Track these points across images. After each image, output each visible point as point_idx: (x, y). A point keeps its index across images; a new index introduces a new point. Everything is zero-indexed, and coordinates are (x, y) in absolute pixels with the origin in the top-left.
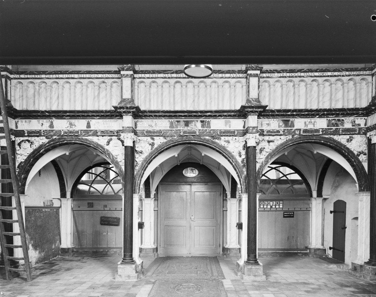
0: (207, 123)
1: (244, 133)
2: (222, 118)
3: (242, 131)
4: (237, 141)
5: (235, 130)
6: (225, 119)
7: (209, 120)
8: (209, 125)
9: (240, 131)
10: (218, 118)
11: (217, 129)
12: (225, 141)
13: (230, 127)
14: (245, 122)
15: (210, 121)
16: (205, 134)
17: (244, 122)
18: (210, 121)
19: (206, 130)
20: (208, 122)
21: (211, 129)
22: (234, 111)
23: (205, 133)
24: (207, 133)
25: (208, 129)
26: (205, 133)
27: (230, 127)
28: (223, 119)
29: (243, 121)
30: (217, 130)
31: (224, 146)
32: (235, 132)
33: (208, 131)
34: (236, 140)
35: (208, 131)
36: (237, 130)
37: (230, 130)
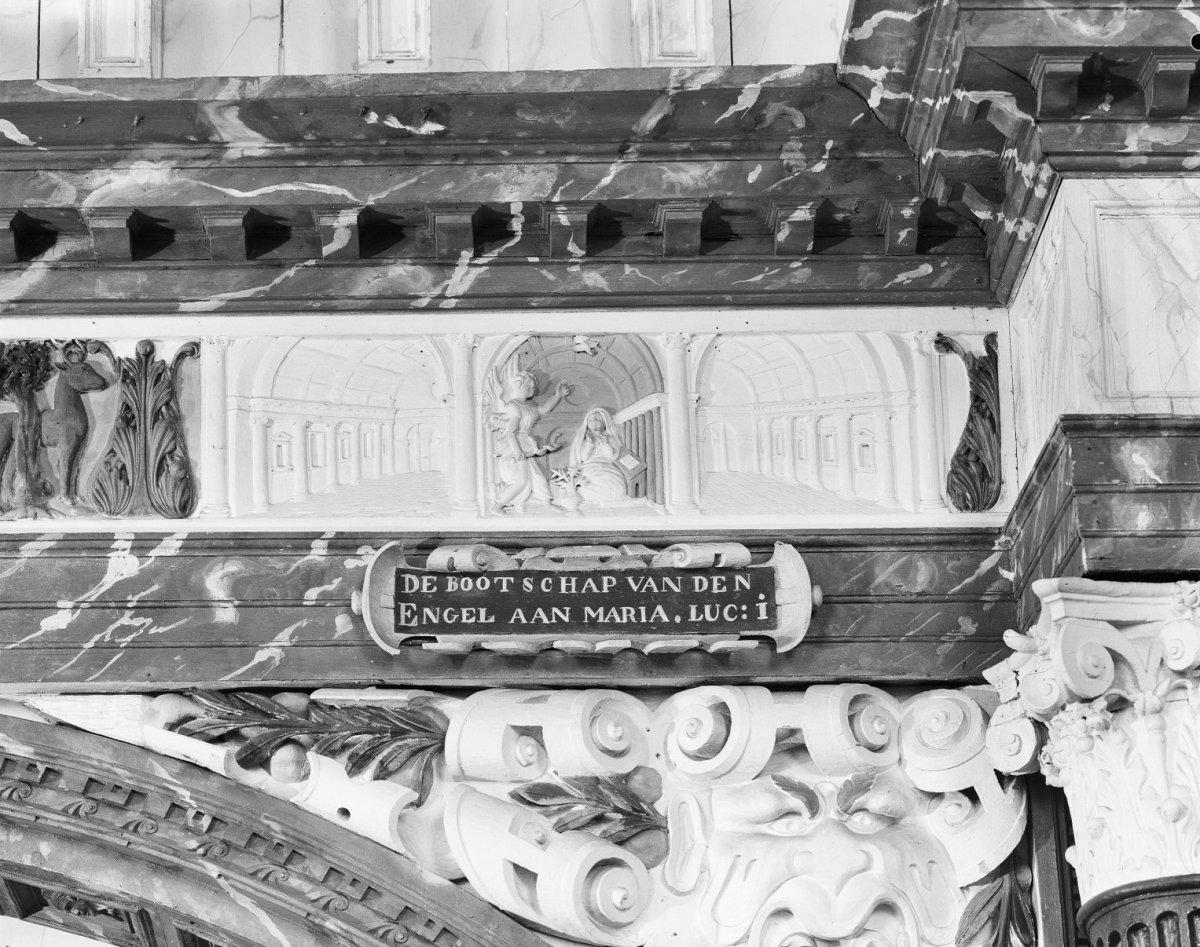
0: (103, 406)
1: (971, 599)
2: (464, 277)
3: (923, 575)
4: (828, 786)
5: (761, 544)
6: (516, 301)
7: (168, 334)
8: (156, 439)
9: (886, 571)
10: (368, 281)
11: (332, 526)
12: (536, 796)
13: (643, 484)
14: (984, 371)
15: (192, 350)
16: (64, 643)
17: (957, 370)
18: (192, 350)
19: (70, 543)
20: (143, 366)
21: (211, 516)
22: (722, 94)
23: (59, 621)
24: (114, 602)
25: (125, 527)
26: (59, 621)
27: (643, 484)
28: (477, 301)
29: (944, 344)
30: (345, 543)
31: (503, 893)
32: (765, 582)
33: (122, 566)
34: (795, 772)
35: (122, 566)
36: (812, 545)
37: (659, 544)
